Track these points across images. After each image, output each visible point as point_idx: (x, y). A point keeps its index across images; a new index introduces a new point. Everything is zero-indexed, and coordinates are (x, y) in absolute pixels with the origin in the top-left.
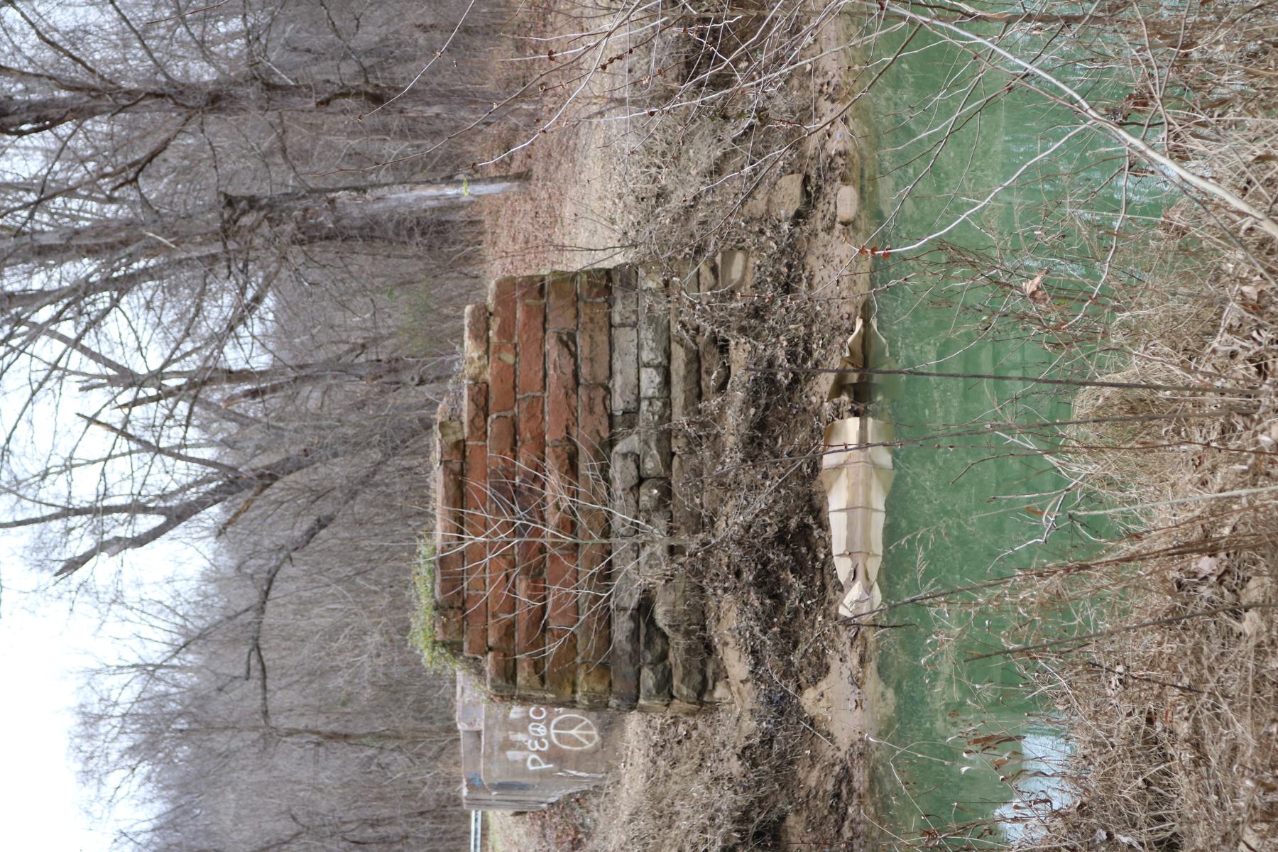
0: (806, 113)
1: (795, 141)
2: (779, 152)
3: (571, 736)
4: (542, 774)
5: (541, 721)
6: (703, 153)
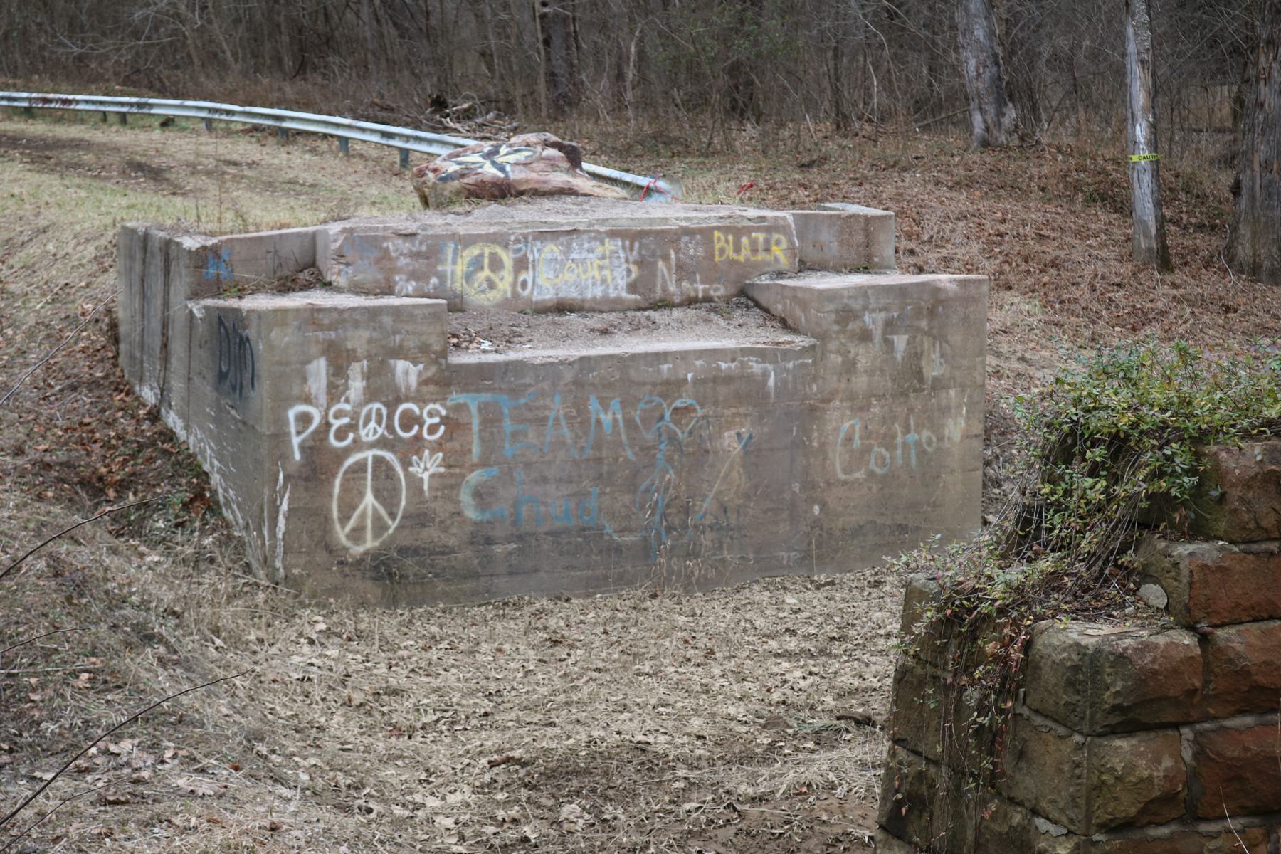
3: (361, 495)
4: (281, 437)
5: (390, 428)
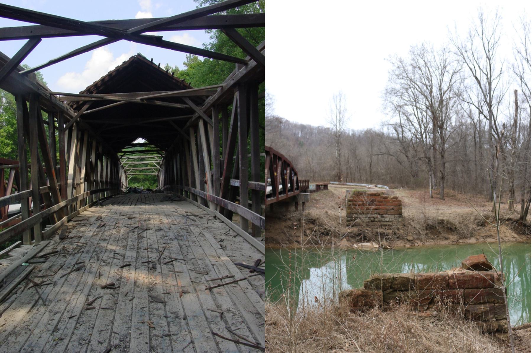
0: (421, 241)
1: (417, 239)
2: (416, 237)
6: (418, 226)
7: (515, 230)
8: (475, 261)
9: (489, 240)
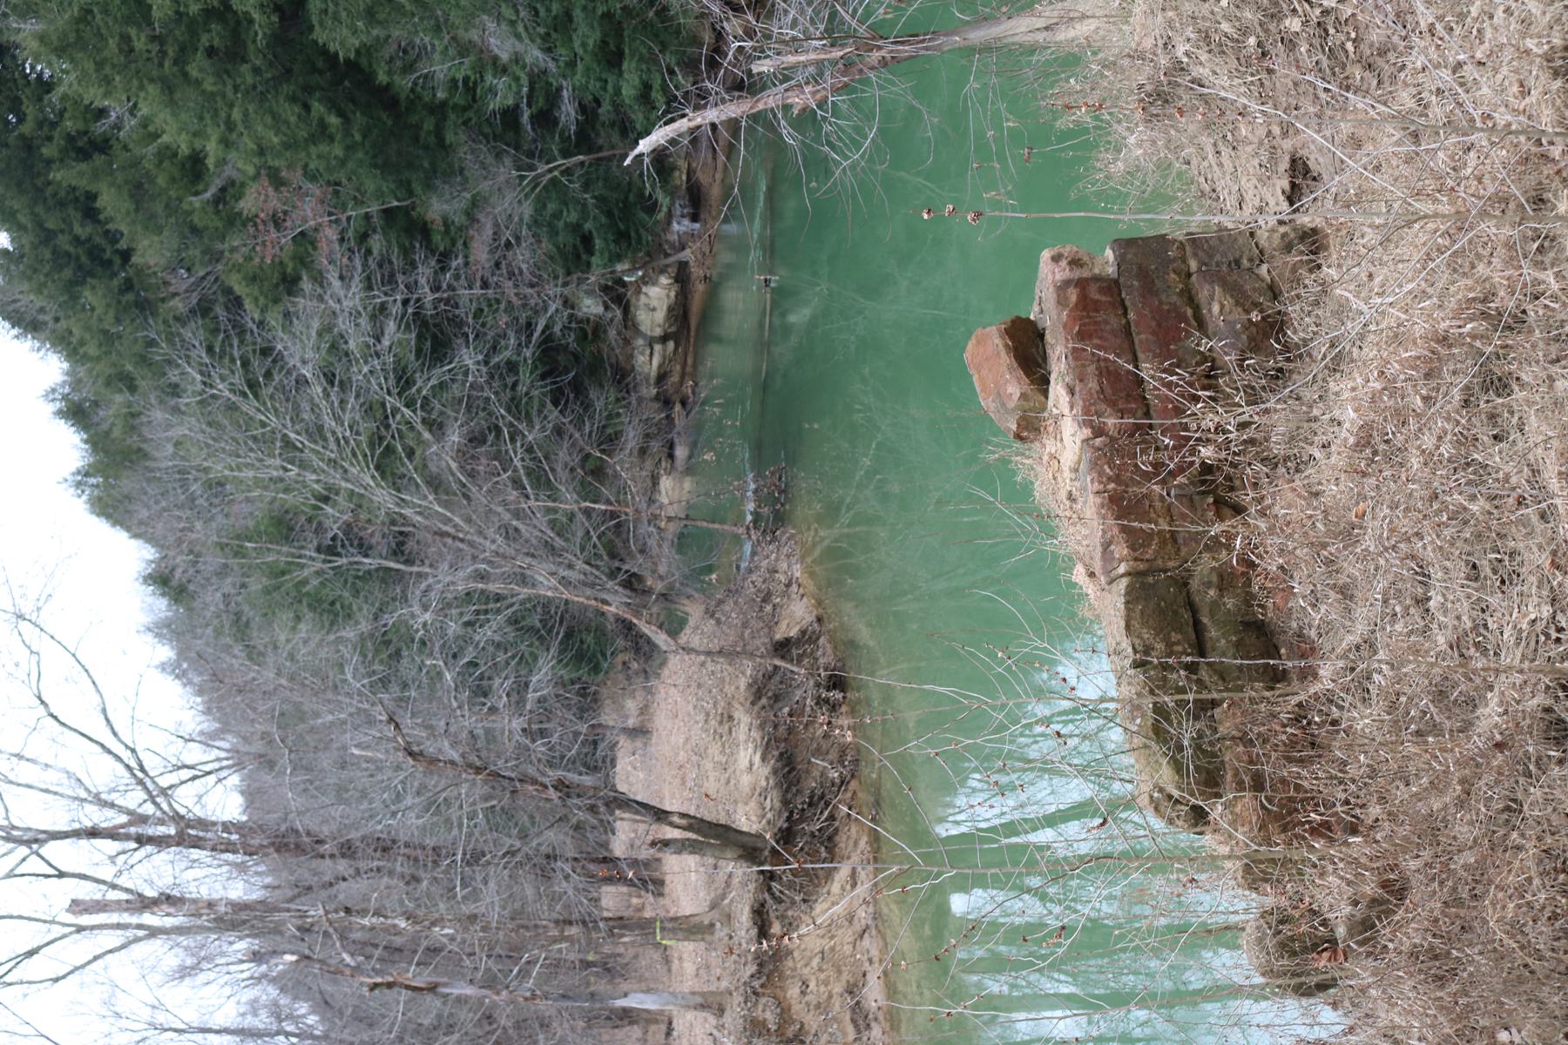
7: (810, 885)
8: (1006, 359)
9: (874, 995)
